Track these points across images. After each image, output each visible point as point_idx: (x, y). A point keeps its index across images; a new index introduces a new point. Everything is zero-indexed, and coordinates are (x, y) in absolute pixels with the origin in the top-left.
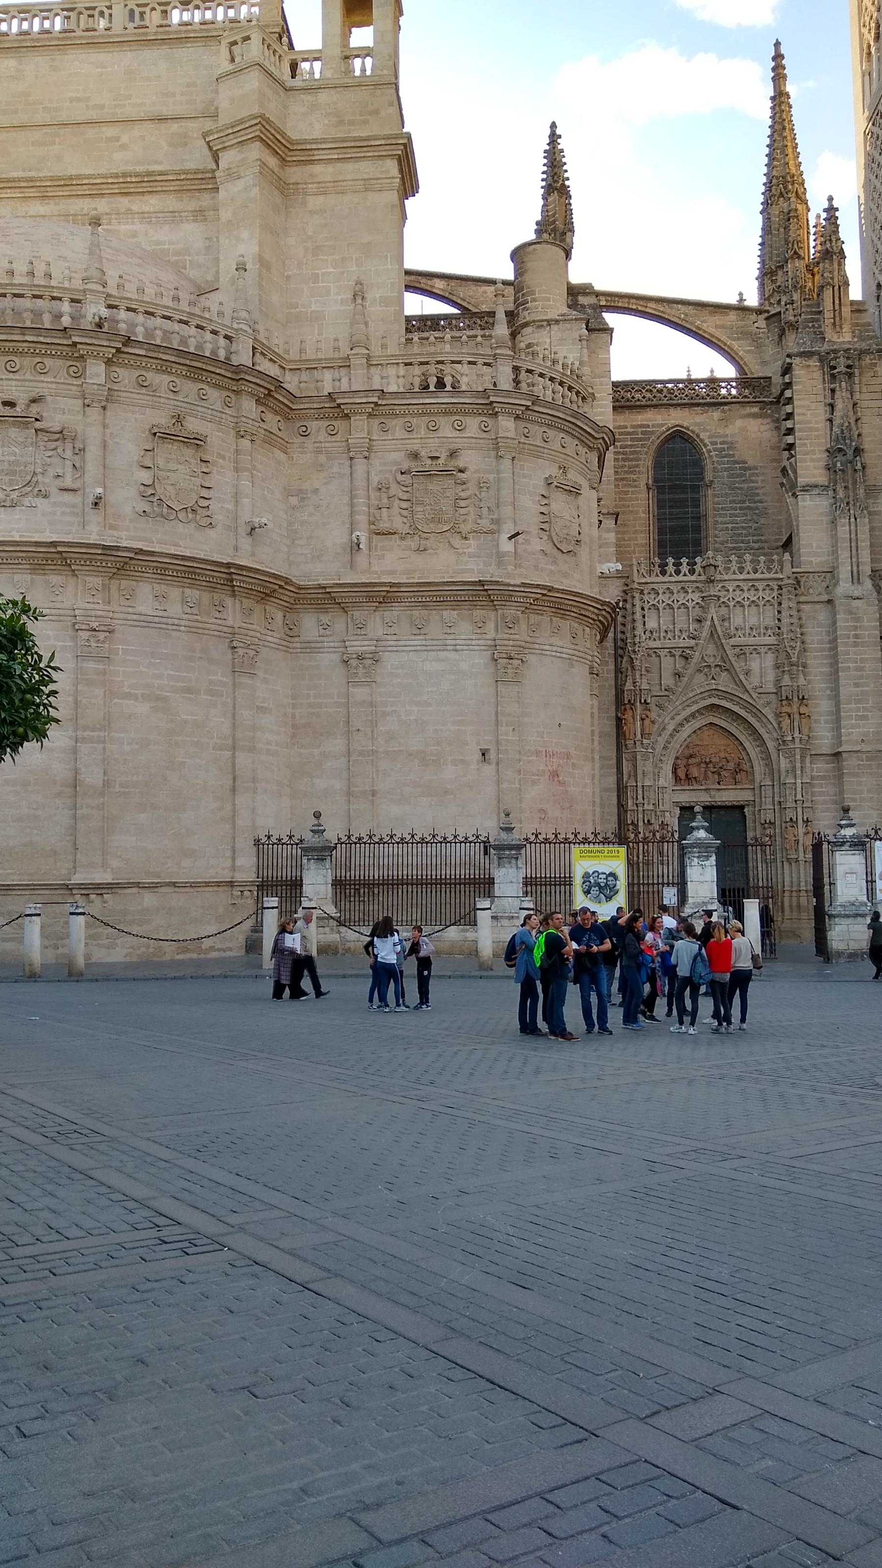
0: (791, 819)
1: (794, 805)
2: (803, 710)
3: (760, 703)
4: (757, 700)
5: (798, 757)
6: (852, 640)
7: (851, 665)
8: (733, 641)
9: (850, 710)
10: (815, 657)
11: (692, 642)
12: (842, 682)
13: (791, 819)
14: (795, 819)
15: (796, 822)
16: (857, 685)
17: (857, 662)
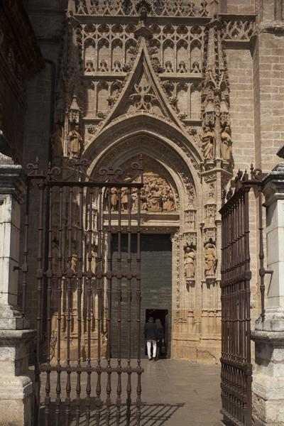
0: (211, 239)
1: (214, 226)
2: (225, 135)
3: (185, 131)
4: (182, 127)
5: (219, 179)
6: (272, 70)
7: (271, 94)
8: (161, 75)
9: (270, 136)
10: (237, 94)
11: (124, 74)
12: (263, 109)
13: (211, 239)
14: (214, 240)
15: (214, 243)
16: (276, 113)
17: (276, 91)
